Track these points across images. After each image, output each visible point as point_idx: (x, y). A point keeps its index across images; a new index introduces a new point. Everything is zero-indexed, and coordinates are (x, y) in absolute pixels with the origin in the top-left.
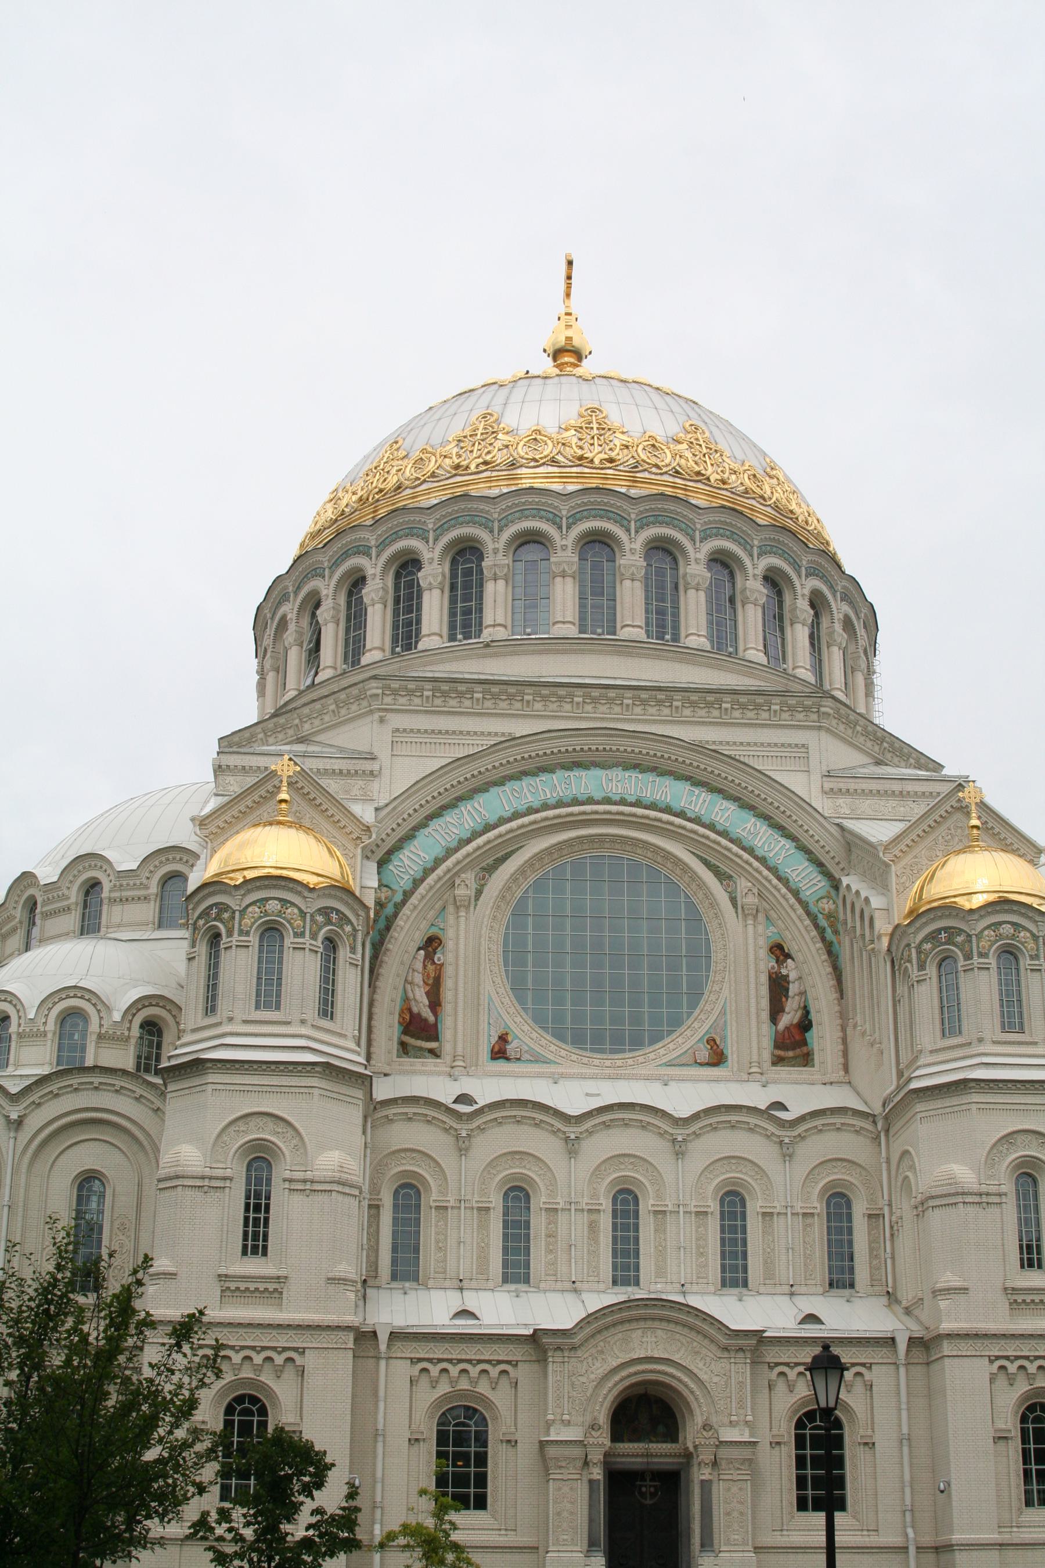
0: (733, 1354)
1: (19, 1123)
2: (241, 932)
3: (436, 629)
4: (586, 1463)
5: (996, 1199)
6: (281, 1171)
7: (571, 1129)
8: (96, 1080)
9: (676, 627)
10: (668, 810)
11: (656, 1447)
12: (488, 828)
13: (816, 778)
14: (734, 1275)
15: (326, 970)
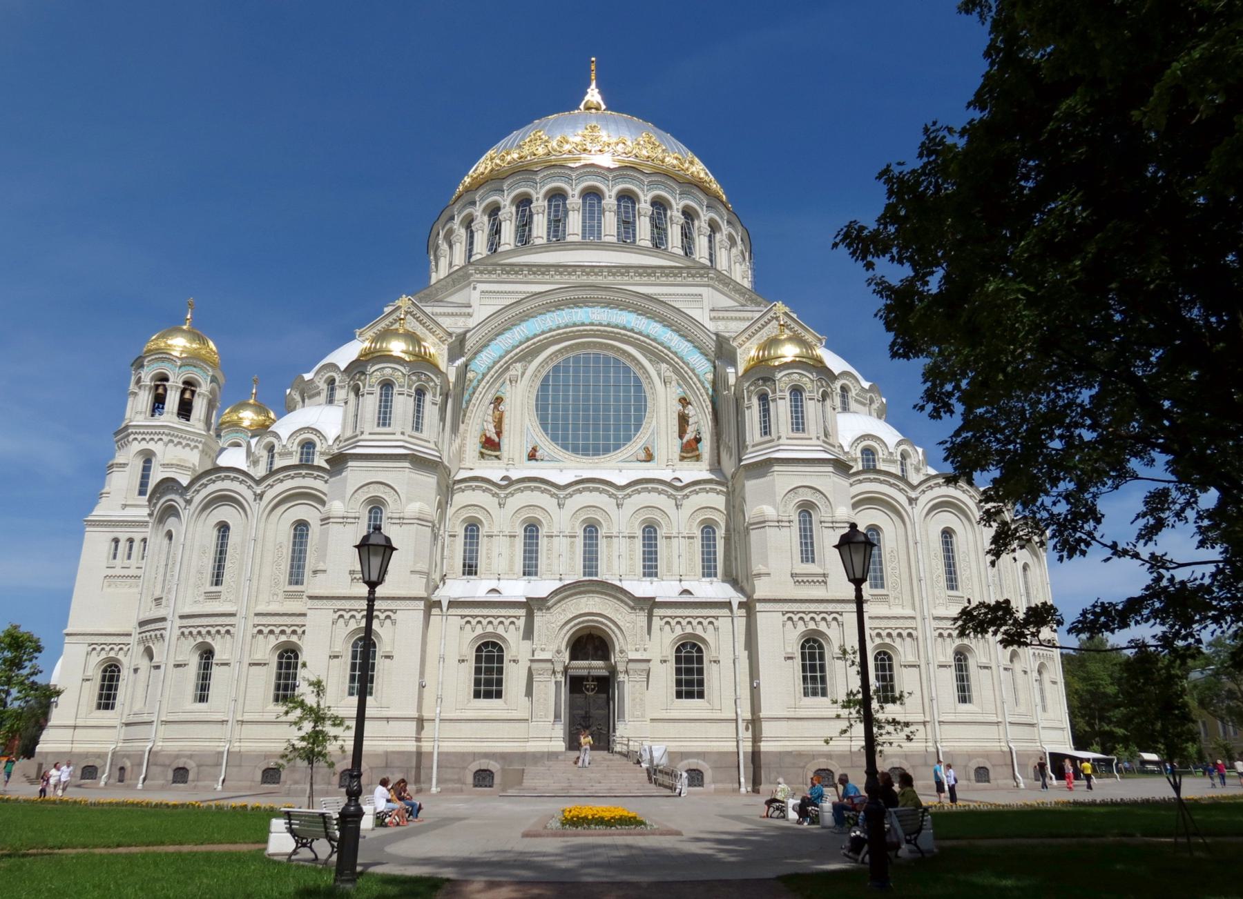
1: (261, 496)
2: (370, 386)
4: (554, 672)
6: (386, 513)
8: (316, 473)
9: (634, 236)
10: (624, 328)
12: (528, 339)
13: (707, 311)
14: (650, 570)
15: (419, 406)
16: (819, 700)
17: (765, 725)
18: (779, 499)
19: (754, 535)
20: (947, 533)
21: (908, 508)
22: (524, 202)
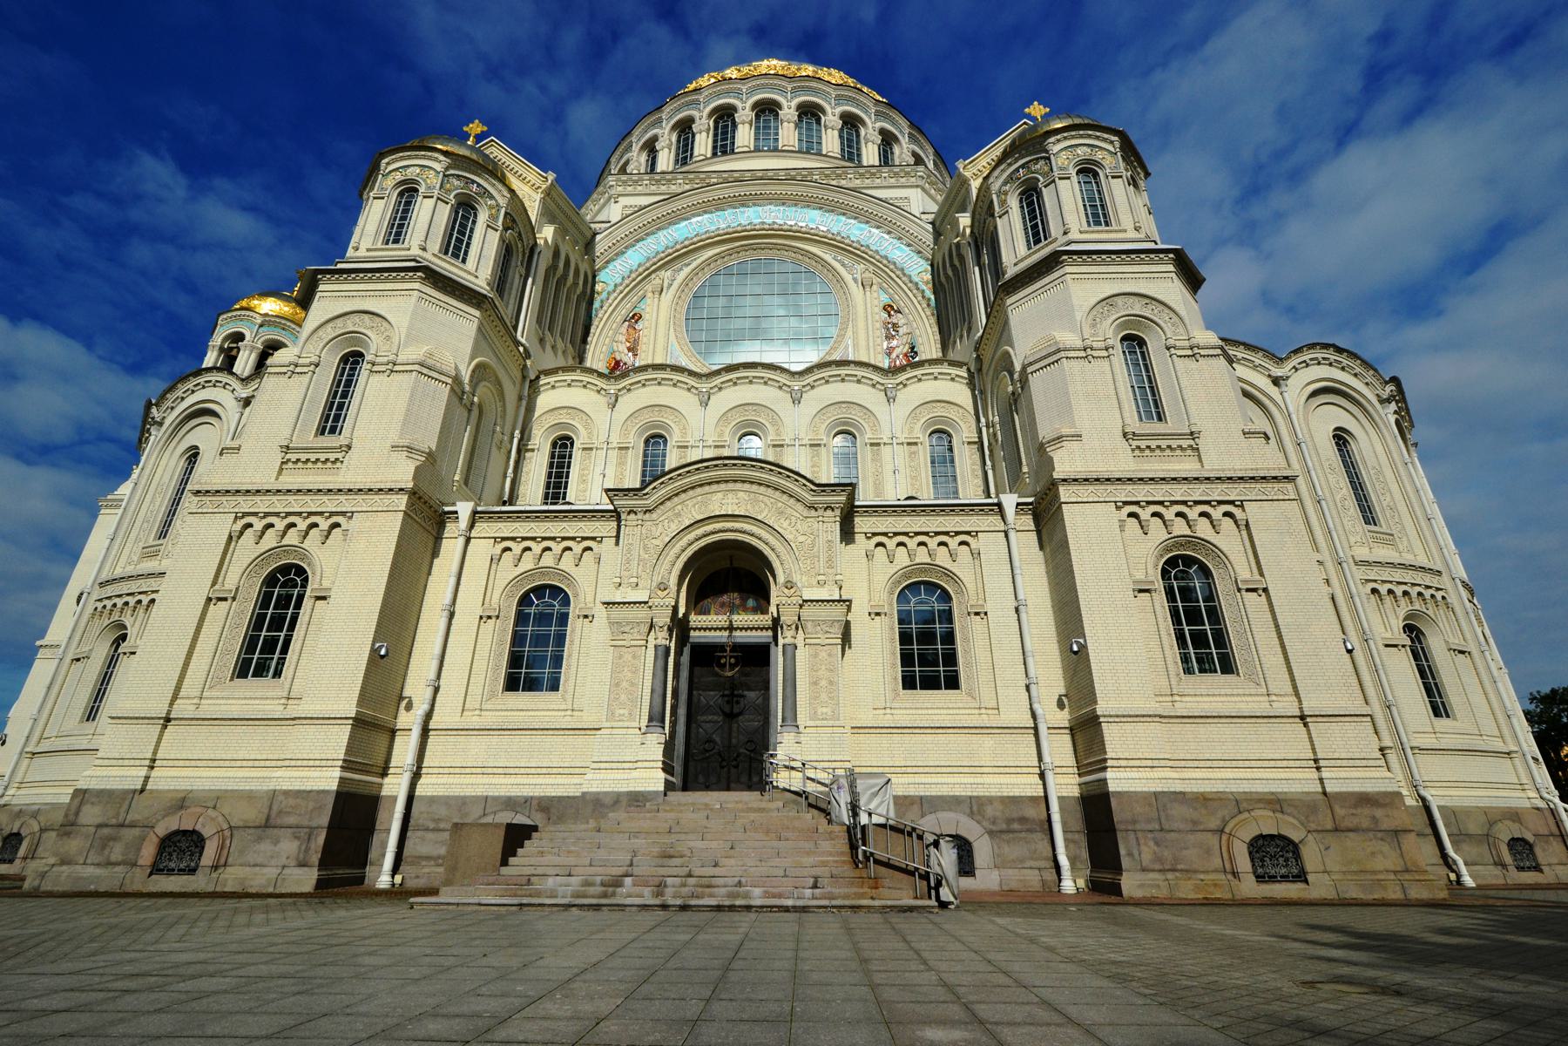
0: (821, 512)
5: (1105, 353)
11: (740, 619)
16: (1218, 680)
17: (1110, 732)
18: (1079, 315)
20: (1341, 438)
21: (1273, 391)
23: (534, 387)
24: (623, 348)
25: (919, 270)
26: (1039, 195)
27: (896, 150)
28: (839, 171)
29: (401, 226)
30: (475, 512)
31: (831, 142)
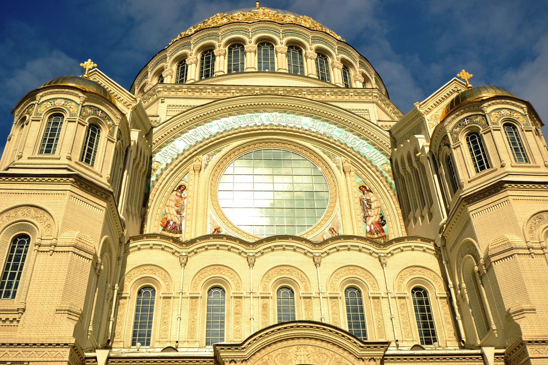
3: (193, 77)
5: (541, 252)
7: (250, 251)
18: (521, 225)
19: (499, 268)
22: (208, 52)
23: (127, 252)
24: (173, 211)
25: (382, 162)
26: (480, 138)
27: (352, 72)
28: (320, 90)
29: (51, 141)
30: (109, 358)
31: (310, 67)
